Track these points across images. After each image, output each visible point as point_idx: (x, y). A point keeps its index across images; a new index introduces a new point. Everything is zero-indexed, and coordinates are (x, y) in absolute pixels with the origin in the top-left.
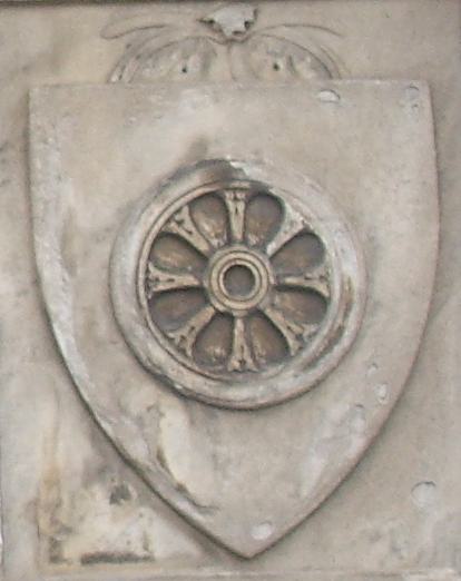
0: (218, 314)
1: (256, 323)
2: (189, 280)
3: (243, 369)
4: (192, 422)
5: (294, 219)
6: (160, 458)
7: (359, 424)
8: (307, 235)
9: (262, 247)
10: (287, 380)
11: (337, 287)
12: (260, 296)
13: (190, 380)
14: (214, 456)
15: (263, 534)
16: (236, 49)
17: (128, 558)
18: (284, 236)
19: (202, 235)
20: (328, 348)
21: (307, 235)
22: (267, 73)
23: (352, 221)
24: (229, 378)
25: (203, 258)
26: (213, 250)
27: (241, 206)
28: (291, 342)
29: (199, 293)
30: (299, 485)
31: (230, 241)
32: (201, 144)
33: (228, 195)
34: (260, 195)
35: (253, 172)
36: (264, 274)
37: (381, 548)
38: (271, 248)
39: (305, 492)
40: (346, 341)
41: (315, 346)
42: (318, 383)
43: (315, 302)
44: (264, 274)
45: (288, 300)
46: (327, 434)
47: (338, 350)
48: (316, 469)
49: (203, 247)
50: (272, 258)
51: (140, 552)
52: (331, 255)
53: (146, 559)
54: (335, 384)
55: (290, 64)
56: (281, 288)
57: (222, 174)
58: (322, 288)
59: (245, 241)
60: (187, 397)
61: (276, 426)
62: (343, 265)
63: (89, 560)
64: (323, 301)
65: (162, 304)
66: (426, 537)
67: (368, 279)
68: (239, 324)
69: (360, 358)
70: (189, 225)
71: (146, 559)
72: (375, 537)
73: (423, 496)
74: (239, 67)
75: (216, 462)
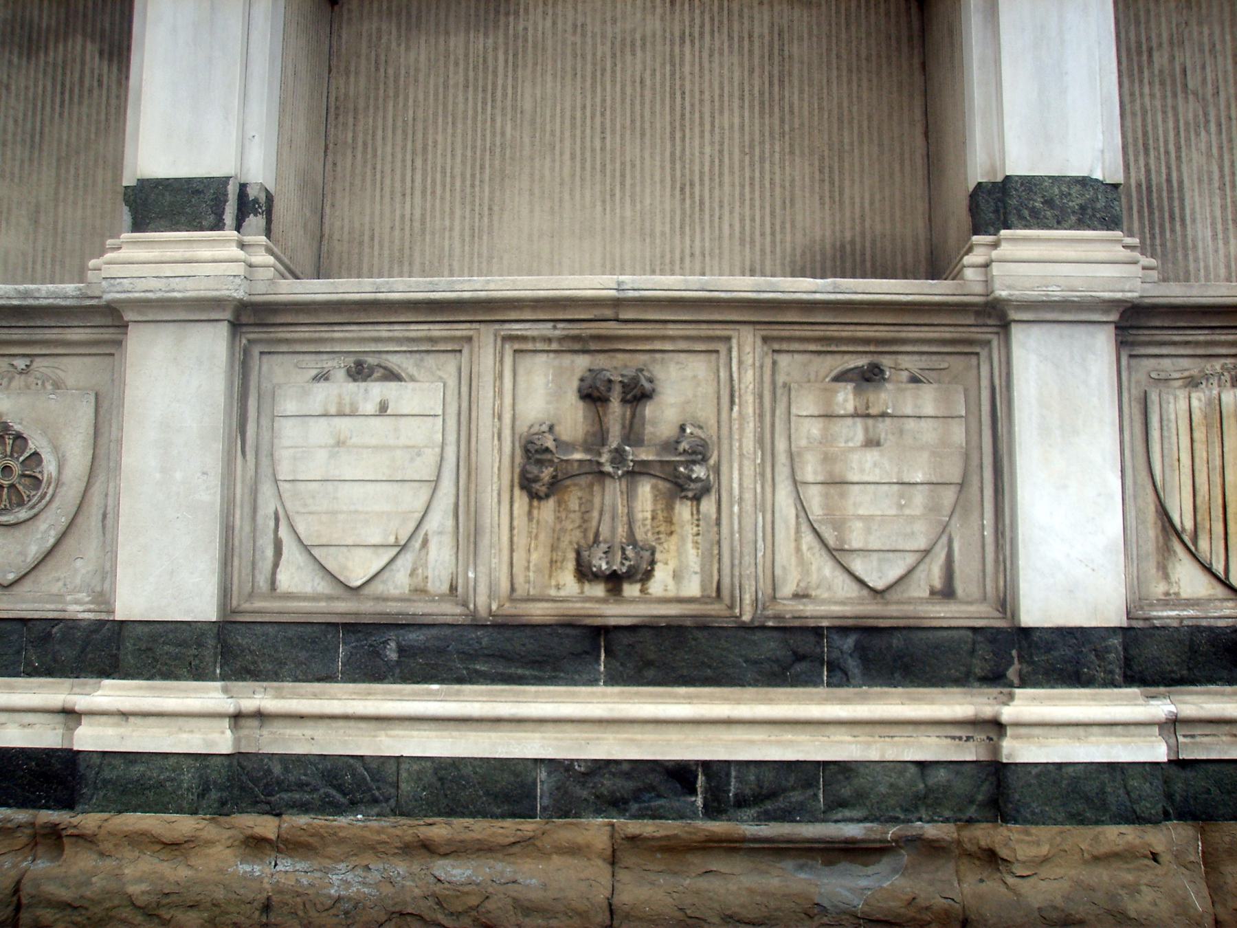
3: (5, 509)
5: (32, 446)
7: (53, 533)
8: (36, 454)
9: (17, 458)
10: (23, 514)
12: (14, 479)
15: (11, 577)
16: (23, 377)
18: (26, 455)
20: (40, 501)
21: (36, 454)
22: (33, 387)
23: (56, 449)
30: (26, 556)
34: (19, 437)
35: (17, 427)
36: (17, 469)
37: (60, 584)
38: (21, 459)
39: (28, 560)
40: (48, 498)
41: (34, 500)
42: (36, 515)
43: (37, 483)
44: (17, 469)
45: (27, 481)
46: (39, 536)
47: (44, 502)
48: (34, 551)
52: (45, 462)
54: (43, 516)
55: (43, 384)
56: (24, 476)
58: (39, 476)
59: (12, 456)
61: (18, 533)
62: (49, 466)
64: (39, 481)
66: (78, 581)
67: (59, 472)
69: (54, 505)
72: (58, 580)
73: (79, 563)
74: (23, 384)
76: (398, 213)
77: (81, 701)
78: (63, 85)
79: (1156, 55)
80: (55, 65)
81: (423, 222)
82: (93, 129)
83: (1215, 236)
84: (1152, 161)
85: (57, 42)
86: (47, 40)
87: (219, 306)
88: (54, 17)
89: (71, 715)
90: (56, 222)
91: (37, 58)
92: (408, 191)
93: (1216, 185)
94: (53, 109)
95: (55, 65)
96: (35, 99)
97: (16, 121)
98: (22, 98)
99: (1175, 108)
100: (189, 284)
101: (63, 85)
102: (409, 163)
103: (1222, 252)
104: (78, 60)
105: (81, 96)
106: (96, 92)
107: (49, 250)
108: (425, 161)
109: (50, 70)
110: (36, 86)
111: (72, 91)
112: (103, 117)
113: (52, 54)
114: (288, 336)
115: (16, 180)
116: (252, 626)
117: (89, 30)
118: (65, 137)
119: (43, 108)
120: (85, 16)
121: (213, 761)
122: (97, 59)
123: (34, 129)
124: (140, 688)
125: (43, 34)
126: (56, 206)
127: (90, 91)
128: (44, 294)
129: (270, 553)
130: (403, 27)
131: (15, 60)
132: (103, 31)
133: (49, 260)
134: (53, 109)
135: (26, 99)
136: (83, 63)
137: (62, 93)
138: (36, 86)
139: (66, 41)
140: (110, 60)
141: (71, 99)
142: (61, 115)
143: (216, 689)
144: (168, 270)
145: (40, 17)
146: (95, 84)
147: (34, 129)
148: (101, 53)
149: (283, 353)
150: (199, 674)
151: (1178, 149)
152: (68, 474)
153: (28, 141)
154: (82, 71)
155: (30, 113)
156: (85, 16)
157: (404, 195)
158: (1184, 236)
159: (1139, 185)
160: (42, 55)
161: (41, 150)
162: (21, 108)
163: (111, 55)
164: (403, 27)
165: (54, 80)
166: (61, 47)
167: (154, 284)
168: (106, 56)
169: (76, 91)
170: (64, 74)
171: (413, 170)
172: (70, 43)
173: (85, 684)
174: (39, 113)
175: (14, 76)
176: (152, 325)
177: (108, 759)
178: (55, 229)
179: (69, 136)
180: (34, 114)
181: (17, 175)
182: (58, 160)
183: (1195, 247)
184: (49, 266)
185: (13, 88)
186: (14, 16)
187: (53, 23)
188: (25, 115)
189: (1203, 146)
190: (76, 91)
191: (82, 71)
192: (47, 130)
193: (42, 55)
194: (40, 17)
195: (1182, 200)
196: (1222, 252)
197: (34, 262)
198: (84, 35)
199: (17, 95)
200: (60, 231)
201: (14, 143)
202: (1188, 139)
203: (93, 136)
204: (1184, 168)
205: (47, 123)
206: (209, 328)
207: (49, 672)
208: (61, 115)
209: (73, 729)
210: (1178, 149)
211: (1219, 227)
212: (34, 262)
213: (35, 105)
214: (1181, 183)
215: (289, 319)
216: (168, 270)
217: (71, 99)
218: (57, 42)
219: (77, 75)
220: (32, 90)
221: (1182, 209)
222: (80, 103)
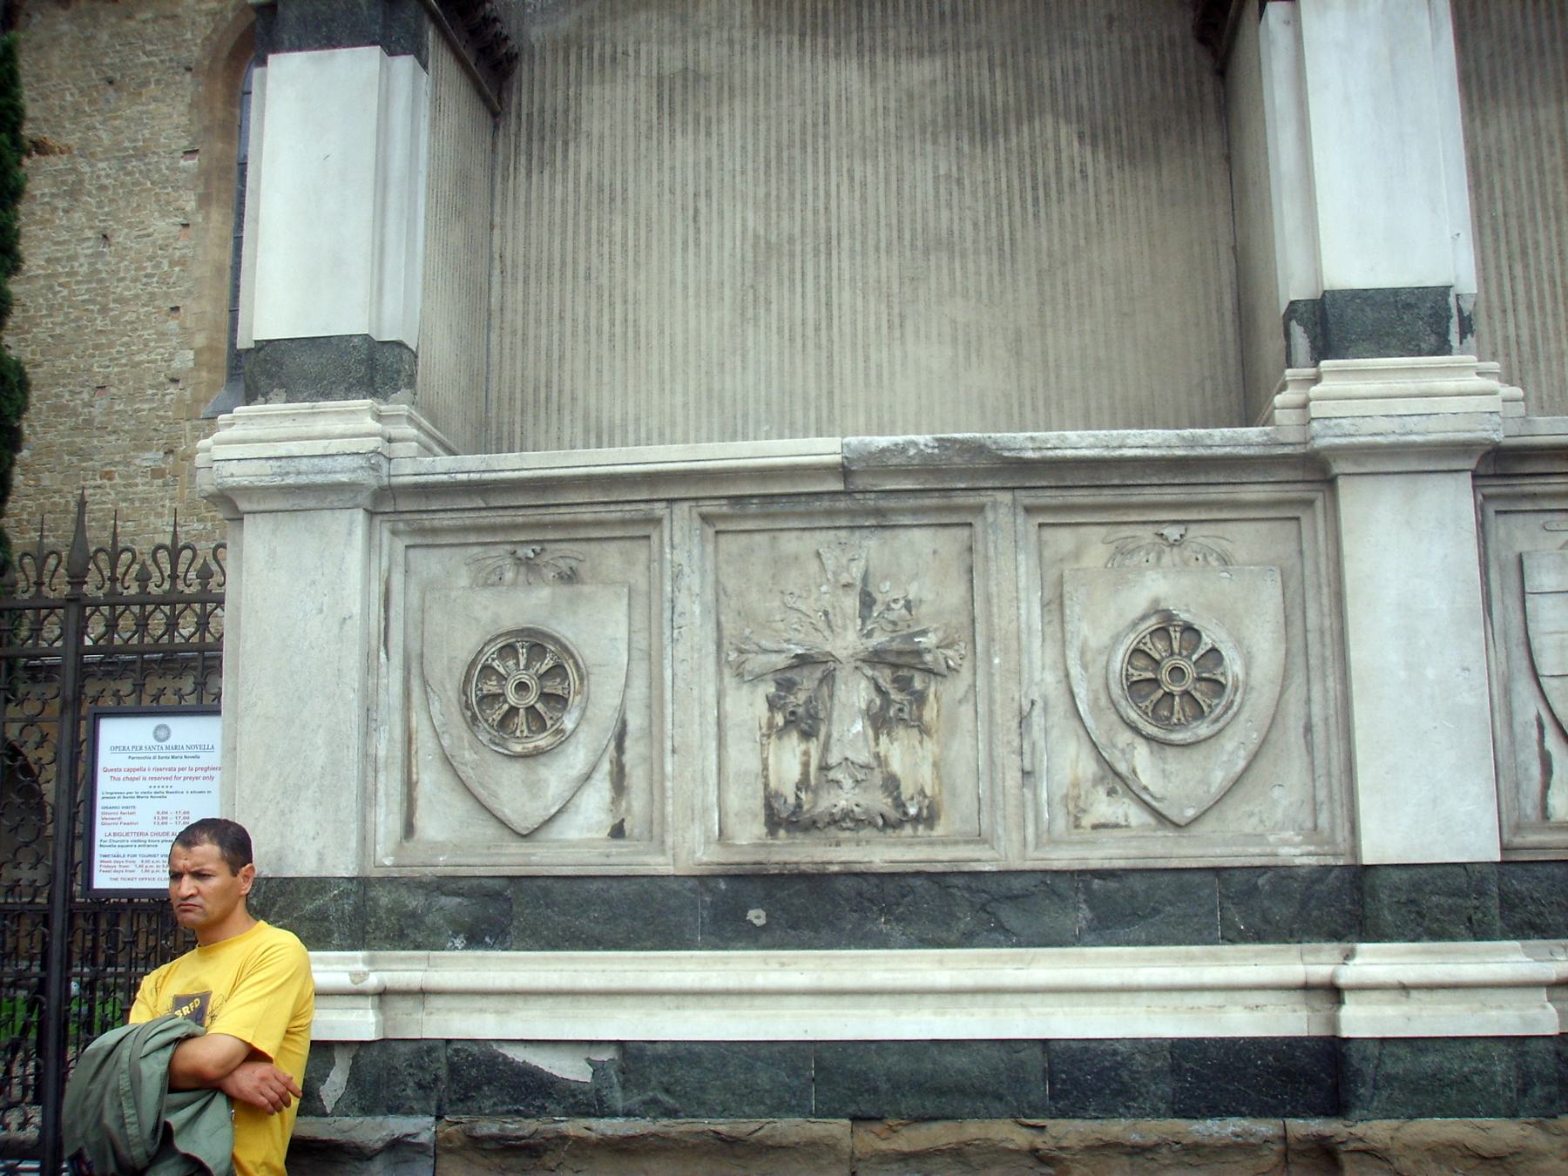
0: (1166, 694)
1: (1186, 698)
2: (1150, 675)
3: (1179, 723)
4: (1152, 752)
5: (1207, 642)
6: (1134, 771)
7: (1242, 753)
8: (1214, 650)
9: (1189, 657)
10: (1203, 729)
11: (1230, 679)
12: (1188, 683)
13: (1150, 730)
14: (1164, 771)
15: (1190, 813)
16: (1175, 550)
17: (1117, 826)
18: (1201, 651)
19: (1158, 649)
20: (1225, 712)
21: (1214, 650)
22: (1193, 562)
23: (1238, 642)
24: (1171, 728)
25: (1157, 663)
26: (1163, 659)
27: (1178, 635)
28: (1205, 708)
29: (1155, 682)
30: (1209, 786)
31: (1172, 654)
32: (1156, 601)
33: (1171, 629)
34: (1188, 628)
35: (1184, 616)
36: (1191, 672)
37: (1254, 820)
38: (1195, 657)
39: (1213, 790)
40: (1235, 708)
41: (1218, 710)
42: (1220, 731)
43: (1218, 687)
44: (1191, 672)
45: (1203, 686)
46: (1225, 758)
47: (1230, 713)
48: (1218, 778)
49: (1157, 657)
50: (1195, 663)
51: (1123, 823)
52: (1227, 661)
53: (1127, 826)
54: (1229, 732)
55: (1205, 558)
56: (1200, 679)
57: (1168, 617)
58: (1222, 679)
59: (1180, 654)
60: (1149, 739)
61: (1197, 754)
62: (1234, 666)
63: (1095, 827)
64: (1223, 686)
65: (1134, 688)
66: (1279, 814)
67: (1247, 674)
68: (1177, 699)
69: (1243, 717)
70: (1150, 645)
71: (1127, 826)
72: (1251, 815)
73: (1277, 792)
74: (1177, 559)
75: (1165, 774)
76: (1499, 334)
77: (1348, 974)
78: (1034, 177)
80: (1020, 153)
81: (1534, 346)
82: (1082, 235)
85: (1019, 123)
86: (1006, 120)
87: (1465, 452)
88: (1011, 93)
89: (1334, 992)
90: (1044, 353)
91: (996, 145)
92: (1509, 306)
94: (1024, 208)
95: (1020, 153)
96: (998, 196)
97: (975, 225)
98: (980, 195)
100: (1432, 424)
101: (1034, 177)
102: (1506, 271)
104: (1051, 145)
105: (1060, 192)
106: (1079, 188)
107: (1040, 390)
108: (1526, 267)
109: (1014, 160)
110: (998, 180)
111: (1046, 184)
112: (1093, 217)
113: (1014, 140)
114: (1538, 489)
115: (986, 301)
116: (1531, 867)
117: (1061, 108)
118: (1045, 243)
119: (1010, 207)
120: (1053, 90)
121: (1533, 1045)
122: (1076, 144)
123: (1001, 234)
124: (1412, 952)
125: (1000, 115)
126: (1043, 335)
127: (1072, 185)
128: (1217, 440)
129: (1535, 770)
130: (1475, 97)
131: (966, 148)
132: (1079, 109)
133: (1041, 404)
134: (1024, 208)
135: (986, 195)
136: (1058, 151)
137: (1035, 188)
138: (998, 180)
139: (1031, 120)
140: (1094, 146)
141: (1047, 195)
142: (1036, 216)
143: (1515, 950)
144: (1400, 406)
145: (994, 93)
146: (1078, 175)
147: (1001, 234)
148: (1081, 137)
149: (1526, 511)
150: (1479, 931)
152: (1257, 676)
153: (995, 248)
154: (1058, 160)
155: (993, 215)
156: (1053, 90)
157: (1504, 311)
160: (1001, 141)
161: (1013, 261)
162: (981, 208)
163: (1094, 137)
164: (1475, 97)
165: (1021, 171)
166: (1025, 128)
167: (1383, 425)
168: (1088, 140)
169: (1053, 185)
170: (1034, 163)
171: (1512, 278)
172: (1037, 124)
173: (1320, 951)
174: (1005, 213)
175: (966, 168)
176: (1371, 478)
177: (1389, 1048)
178: (1045, 362)
179: (1050, 240)
180: (999, 215)
181: (985, 295)
182: (1039, 272)
184: (1042, 411)
185: (967, 182)
186: (958, 93)
187: (1011, 100)
188: (987, 217)
190: (1053, 185)
191: (1058, 160)
192: (1019, 235)
193: (1001, 141)
194: (994, 93)
197: (1021, 405)
198: (1056, 116)
199: (974, 193)
200: (1051, 364)
201: (976, 252)
203: (1082, 242)
205: (1018, 225)
206: (1449, 480)
207: (1260, 938)
208: (1036, 216)
209: (1338, 1009)
212: (1021, 405)
213: (999, 205)
215: (1541, 468)
216: (1400, 406)
217: (1047, 195)
218: (1019, 123)
219: (1051, 165)
220: (992, 185)
222: (1060, 200)
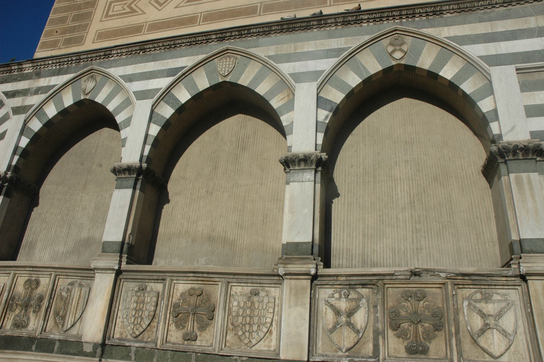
79: (42, 215)
83: (39, 252)
84: (34, 237)
93: (43, 241)
99: (42, 225)
103: (39, 255)
151: (39, 234)
158: (34, 252)
159: (30, 241)
183: (35, 254)
189: (44, 233)
195: (36, 244)
196: (39, 255)
202: (42, 232)
204: (39, 237)
210: (39, 234)
211: (41, 250)
214: (37, 241)
221: (36, 246)
